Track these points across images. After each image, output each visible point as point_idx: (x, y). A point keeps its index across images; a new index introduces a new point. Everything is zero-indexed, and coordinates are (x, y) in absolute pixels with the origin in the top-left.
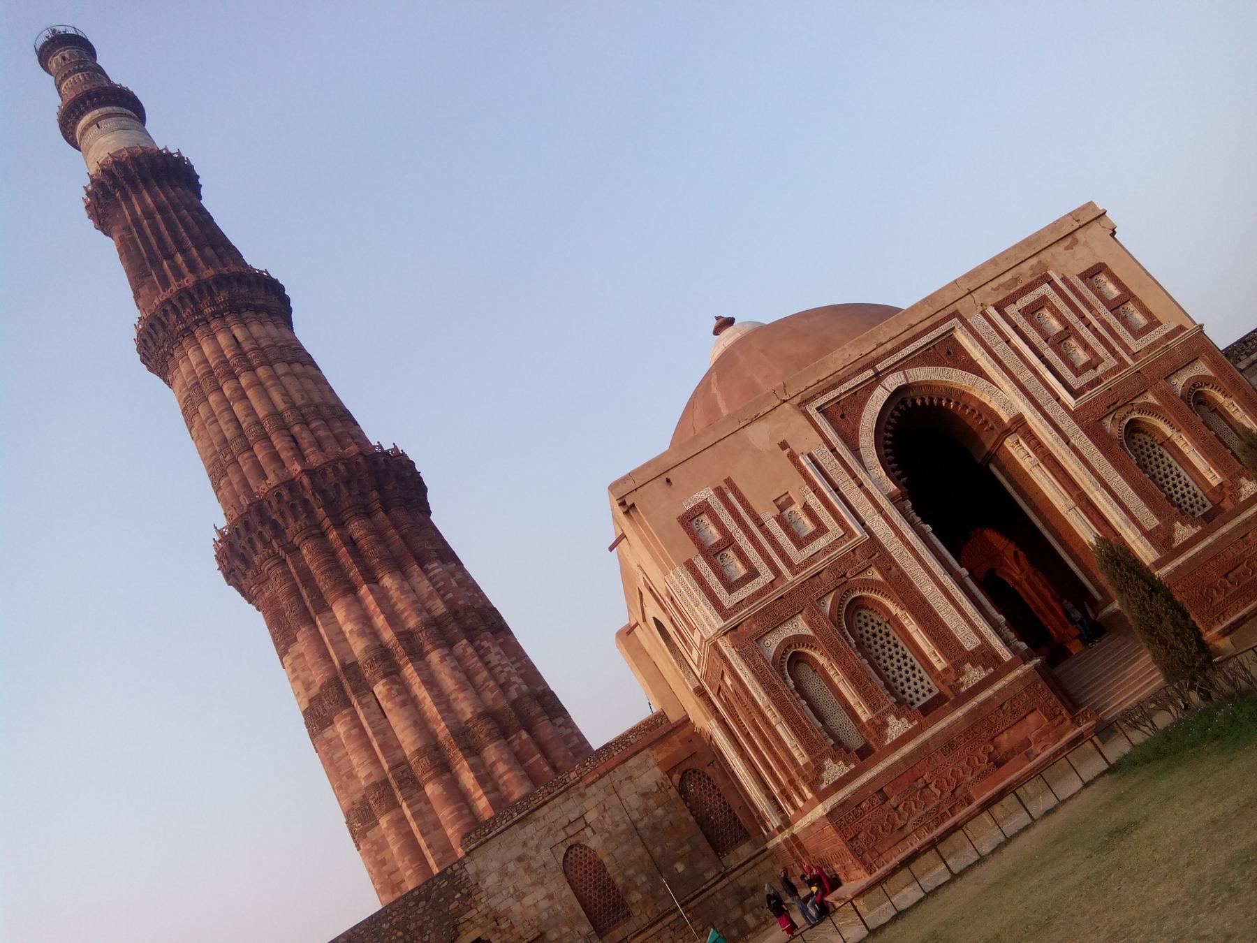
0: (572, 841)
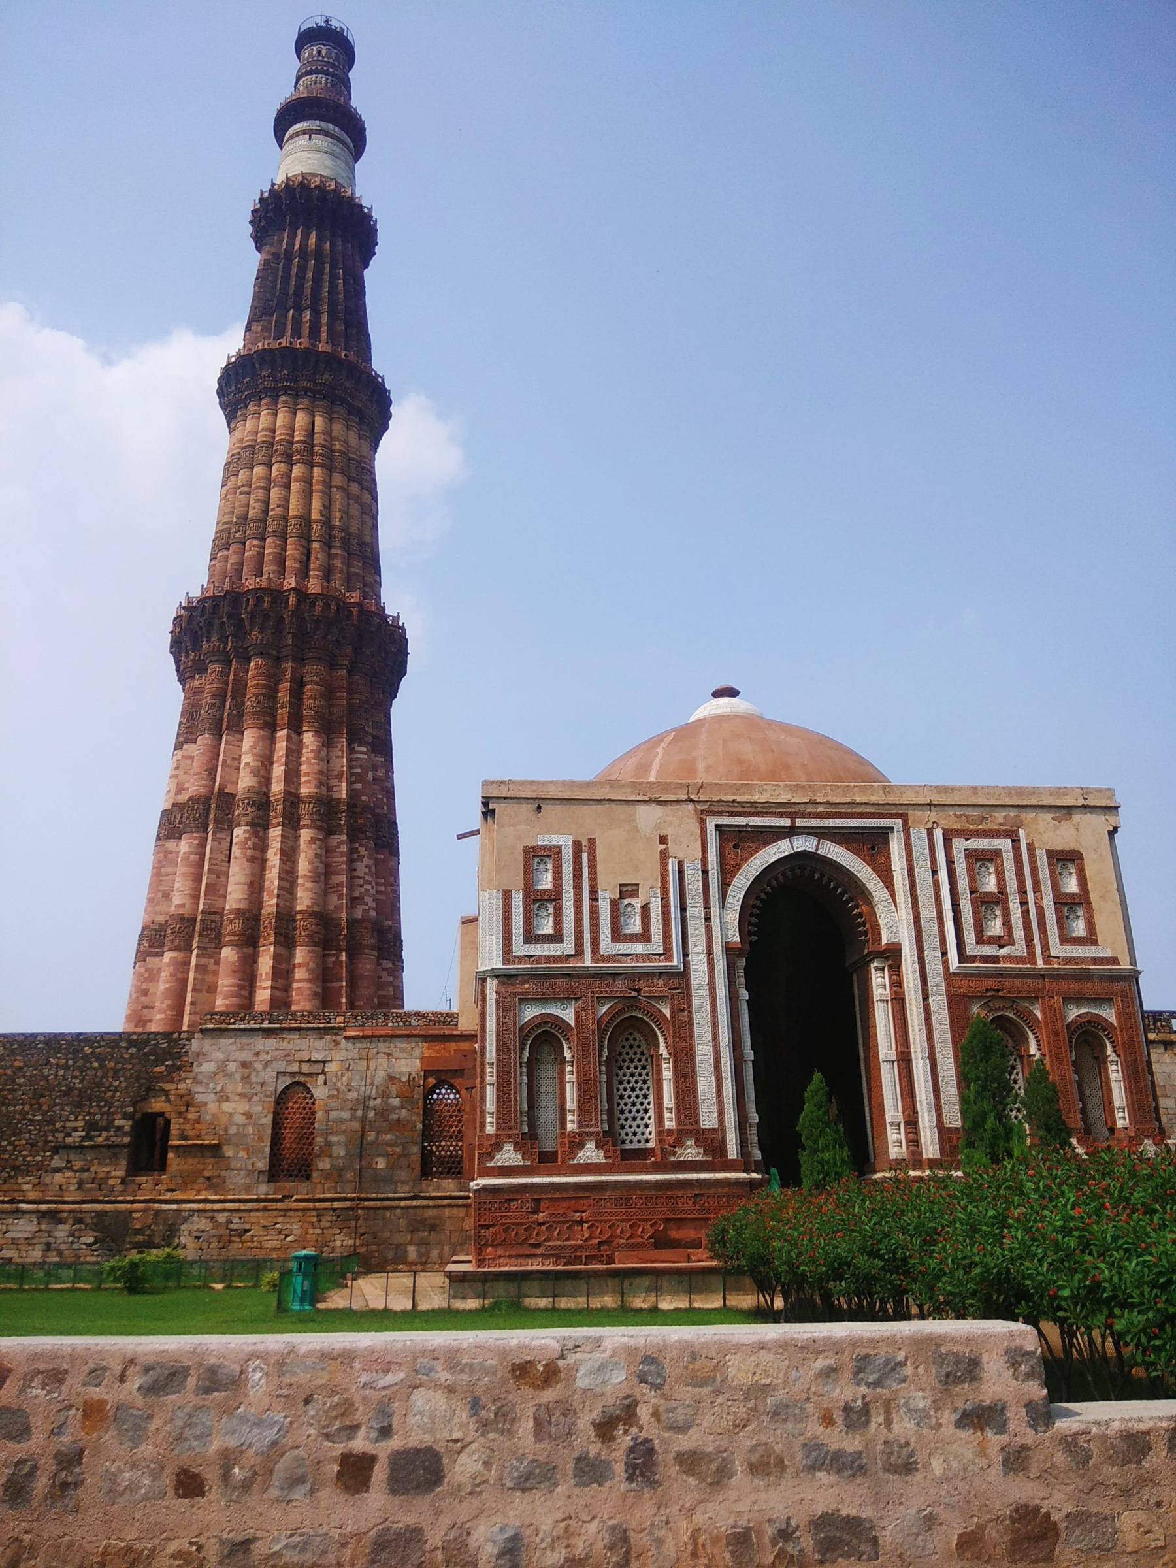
0: (302, 1079)
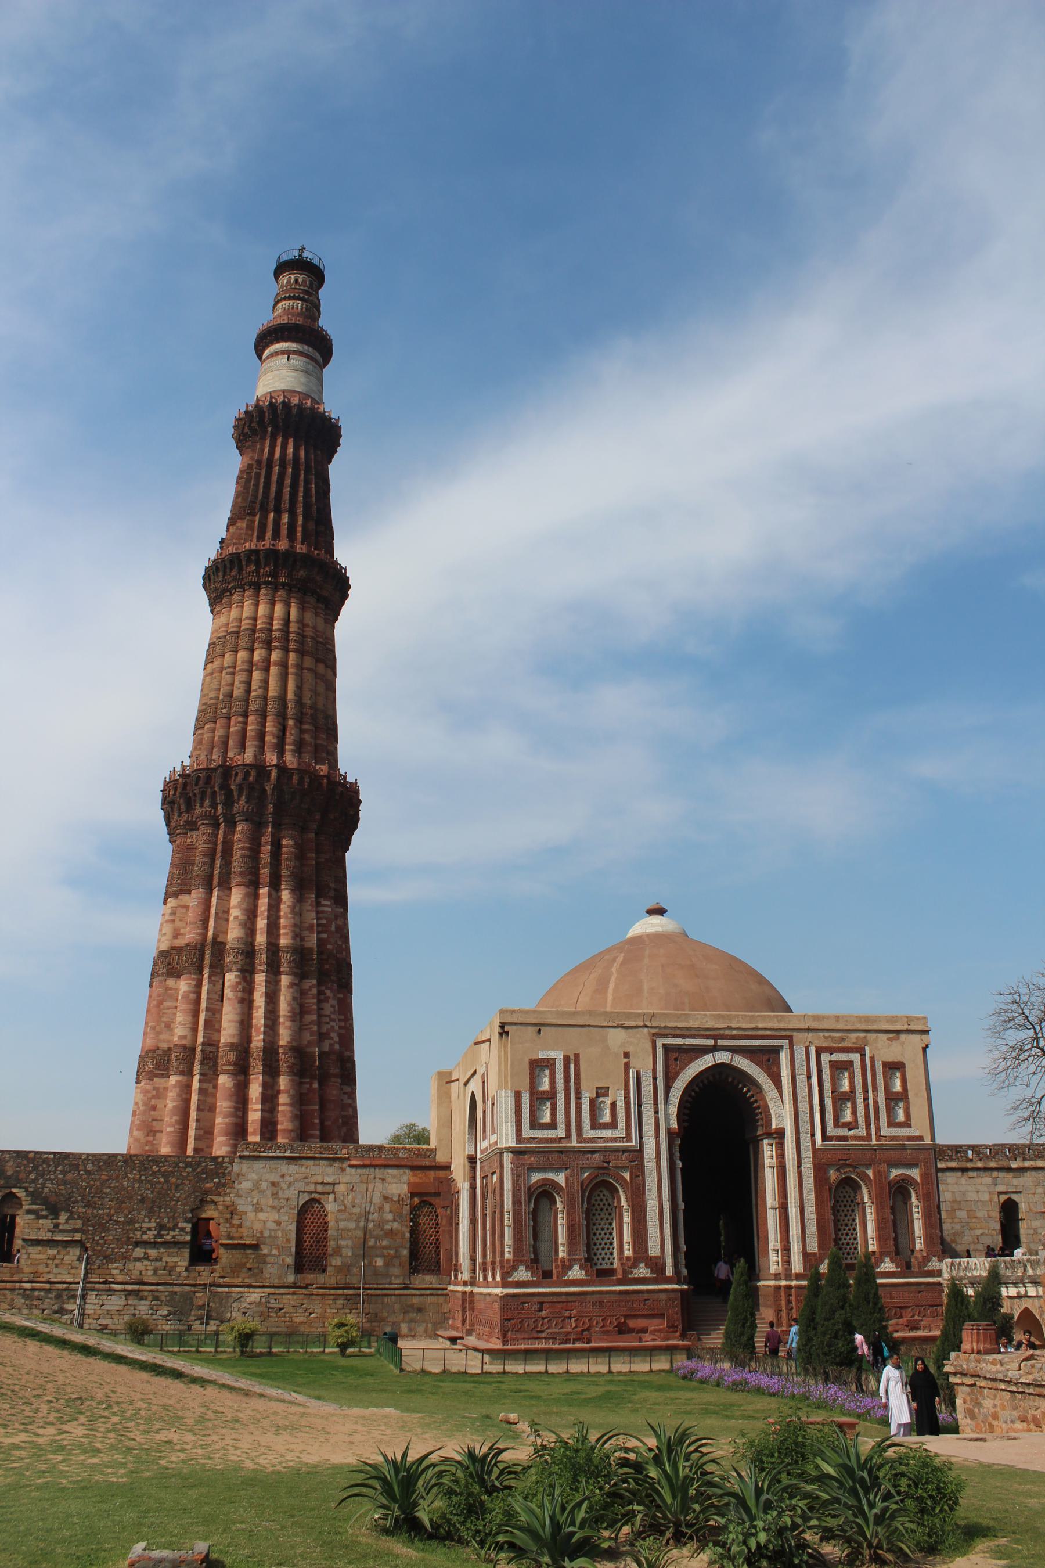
0: (317, 1196)
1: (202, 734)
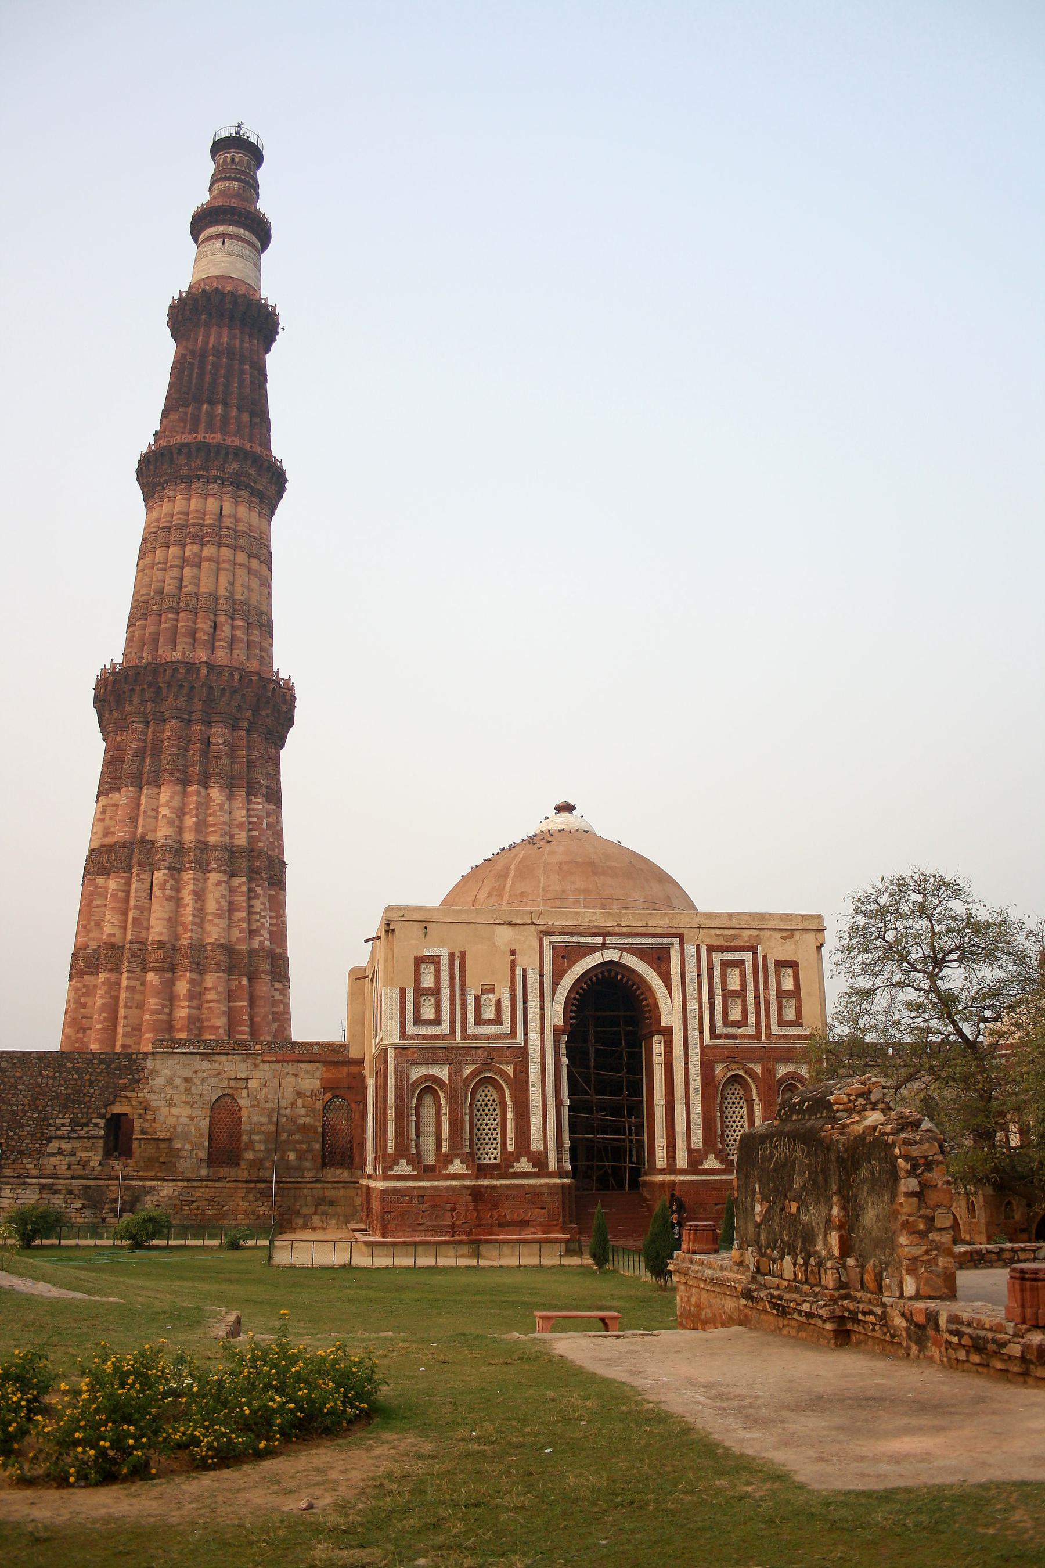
0: (230, 1091)
1: (134, 631)
